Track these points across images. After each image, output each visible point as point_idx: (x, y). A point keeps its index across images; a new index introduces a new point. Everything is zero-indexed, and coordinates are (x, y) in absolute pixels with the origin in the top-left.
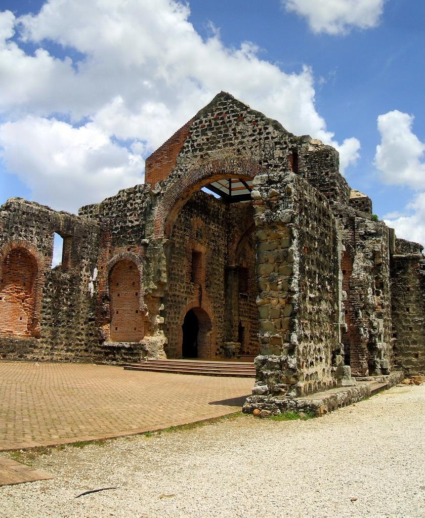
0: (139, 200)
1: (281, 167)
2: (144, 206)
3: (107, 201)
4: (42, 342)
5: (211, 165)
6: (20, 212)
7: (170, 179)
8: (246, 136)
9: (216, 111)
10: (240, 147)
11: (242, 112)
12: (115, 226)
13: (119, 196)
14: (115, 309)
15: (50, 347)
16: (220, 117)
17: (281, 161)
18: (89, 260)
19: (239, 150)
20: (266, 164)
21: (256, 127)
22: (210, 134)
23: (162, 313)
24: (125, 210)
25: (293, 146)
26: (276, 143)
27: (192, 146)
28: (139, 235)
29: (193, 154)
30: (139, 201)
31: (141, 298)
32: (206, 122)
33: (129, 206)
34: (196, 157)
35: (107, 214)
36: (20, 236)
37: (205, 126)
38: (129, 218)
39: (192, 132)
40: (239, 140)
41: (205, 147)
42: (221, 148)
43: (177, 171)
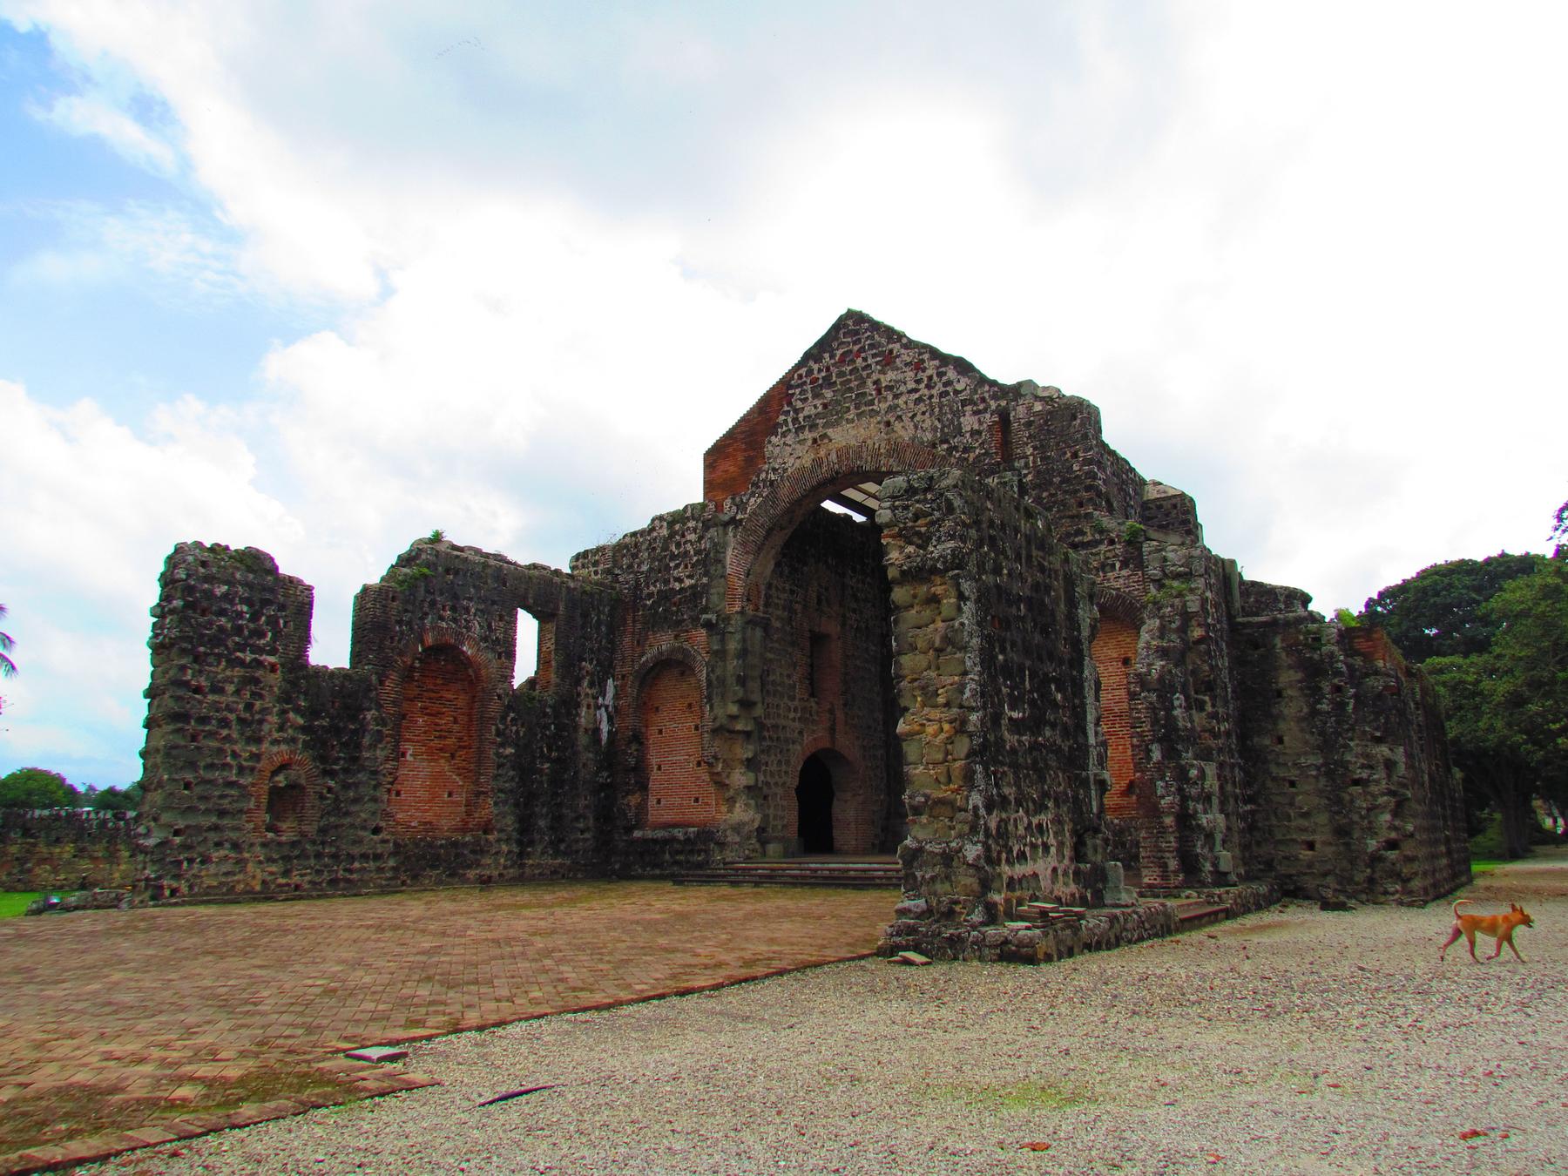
0: (693, 535)
1: (977, 451)
3: (627, 540)
4: (499, 841)
5: (835, 456)
6: (440, 569)
7: (754, 489)
8: (901, 394)
9: (837, 349)
11: (890, 346)
12: (646, 591)
14: (654, 761)
15: (516, 850)
17: (977, 437)
18: (595, 662)
19: (888, 424)
20: (945, 446)
22: (828, 394)
23: (751, 764)
24: (666, 556)
25: (999, 405)
26: (964, 403)
27: (795, 420)
28: (696, 606)
30: (692, 537)
32: (820, 371)
35: (630, 566)
36: (442, 618)
40: (888, 404)
42: (853, 421)
43: (767, 473)
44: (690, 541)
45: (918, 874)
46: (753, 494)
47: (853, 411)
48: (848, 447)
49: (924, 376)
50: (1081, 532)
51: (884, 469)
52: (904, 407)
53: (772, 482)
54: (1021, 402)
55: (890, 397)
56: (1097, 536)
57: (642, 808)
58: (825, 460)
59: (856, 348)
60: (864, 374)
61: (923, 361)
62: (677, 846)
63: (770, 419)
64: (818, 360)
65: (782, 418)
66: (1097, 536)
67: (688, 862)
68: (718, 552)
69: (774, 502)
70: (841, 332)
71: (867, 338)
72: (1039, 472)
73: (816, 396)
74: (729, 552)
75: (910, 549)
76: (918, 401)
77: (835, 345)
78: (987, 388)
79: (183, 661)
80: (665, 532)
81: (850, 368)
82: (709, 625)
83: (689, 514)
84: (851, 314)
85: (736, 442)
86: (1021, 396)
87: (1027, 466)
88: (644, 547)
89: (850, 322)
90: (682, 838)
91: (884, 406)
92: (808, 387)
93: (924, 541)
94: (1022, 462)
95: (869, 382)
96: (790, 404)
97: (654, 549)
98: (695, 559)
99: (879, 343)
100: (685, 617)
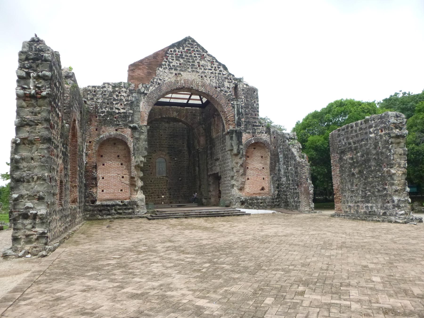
1: (229, 93)
2: (130, 99)
3: (90, 88)
5: (183, 82)
7: (152, 84)
8: (206, 69)
9: (185, 47)
10: (203, 75)
11: (203, 53)
12: (100, 110)
13: (105, 87)
16: (189, 52)
17: (228, 89)
19: (202, 77)
20: (220, 89)
21: (212, 66)
22: (182, 61)
24: (111, 99)
25: (235, 82)
27: (169, 65)
28: (126, 120)
29: (170, 71)
31: (133, 167)
32: (179, 52)
33: (115, 97)
34: (172, 73)
35: (92, 99)
37: (178, 54)
38: (116, 106)
39: (168, 56)
40: (202, 71)
41: (179, 69)
42: (190, 72)
43: (157, 80)
44: (123, 96)
45: (401, 205)
46: (151, 85)
47: (190, 70)
48: (188, 80)
49: (214, 66)
50: (255, 122)
51: (200, 90)
52: (207, 73)
53: (159, 84)
54: (241, 83)
55: (203, 69)
56: (260, 125)
57: (96, 192)
58: (179, 82)
59: (192, 49)
60: (195, 59)
61: (213, 61)
62: (118, 207)
63: (158, 62)
64: (179, 48)
65: (164, 63)
66: (260, 125)
67: (125, 213)
68: (138, 102)
69: (160, 91)
70: (187, 42)
71: (196, 48)
72: (245, 104)
73: (177, 60)
74: (141, 104)
75: (397, 130)
76: (212, 73)
77: (184, 45)
78: (232, 76)
79: (49, 108)
80: (110, 89)
81: (190, 55)
82: (134, 129)
83: (122, 85)
84: (190, 38)
85: (144, 65)
86: (241, 81)
87: (242, 101)
88: (101, 92)
89: (190, 40)
90: (121, 204)
91: (201, 71)
92: (174, 56)
93: (401, 129)
94: (241, 100)
95: (196, 62)
96: (167, 59)
97: (104, 95)
98: (126, 103)
99: (200, 51)
100: (120, 123)
